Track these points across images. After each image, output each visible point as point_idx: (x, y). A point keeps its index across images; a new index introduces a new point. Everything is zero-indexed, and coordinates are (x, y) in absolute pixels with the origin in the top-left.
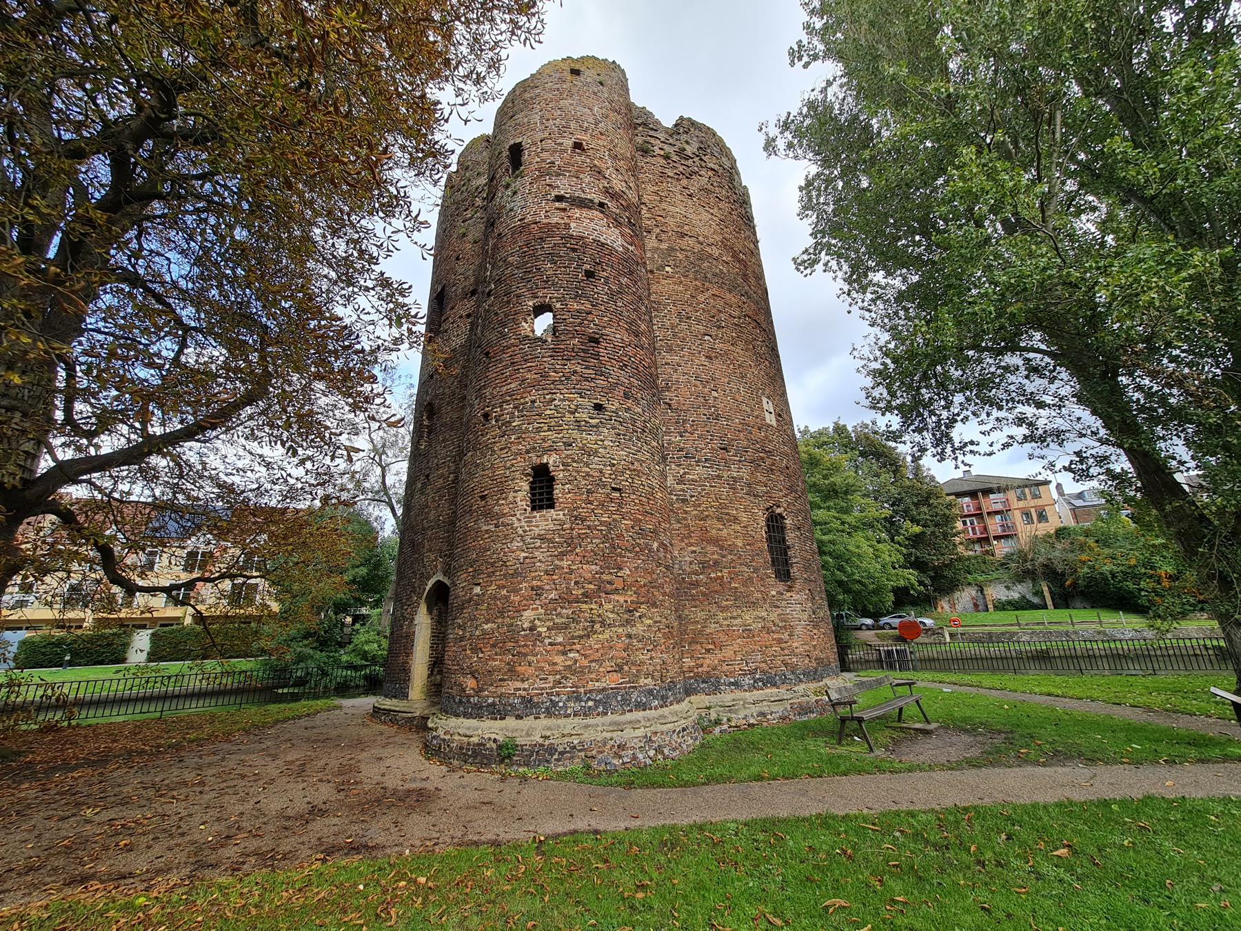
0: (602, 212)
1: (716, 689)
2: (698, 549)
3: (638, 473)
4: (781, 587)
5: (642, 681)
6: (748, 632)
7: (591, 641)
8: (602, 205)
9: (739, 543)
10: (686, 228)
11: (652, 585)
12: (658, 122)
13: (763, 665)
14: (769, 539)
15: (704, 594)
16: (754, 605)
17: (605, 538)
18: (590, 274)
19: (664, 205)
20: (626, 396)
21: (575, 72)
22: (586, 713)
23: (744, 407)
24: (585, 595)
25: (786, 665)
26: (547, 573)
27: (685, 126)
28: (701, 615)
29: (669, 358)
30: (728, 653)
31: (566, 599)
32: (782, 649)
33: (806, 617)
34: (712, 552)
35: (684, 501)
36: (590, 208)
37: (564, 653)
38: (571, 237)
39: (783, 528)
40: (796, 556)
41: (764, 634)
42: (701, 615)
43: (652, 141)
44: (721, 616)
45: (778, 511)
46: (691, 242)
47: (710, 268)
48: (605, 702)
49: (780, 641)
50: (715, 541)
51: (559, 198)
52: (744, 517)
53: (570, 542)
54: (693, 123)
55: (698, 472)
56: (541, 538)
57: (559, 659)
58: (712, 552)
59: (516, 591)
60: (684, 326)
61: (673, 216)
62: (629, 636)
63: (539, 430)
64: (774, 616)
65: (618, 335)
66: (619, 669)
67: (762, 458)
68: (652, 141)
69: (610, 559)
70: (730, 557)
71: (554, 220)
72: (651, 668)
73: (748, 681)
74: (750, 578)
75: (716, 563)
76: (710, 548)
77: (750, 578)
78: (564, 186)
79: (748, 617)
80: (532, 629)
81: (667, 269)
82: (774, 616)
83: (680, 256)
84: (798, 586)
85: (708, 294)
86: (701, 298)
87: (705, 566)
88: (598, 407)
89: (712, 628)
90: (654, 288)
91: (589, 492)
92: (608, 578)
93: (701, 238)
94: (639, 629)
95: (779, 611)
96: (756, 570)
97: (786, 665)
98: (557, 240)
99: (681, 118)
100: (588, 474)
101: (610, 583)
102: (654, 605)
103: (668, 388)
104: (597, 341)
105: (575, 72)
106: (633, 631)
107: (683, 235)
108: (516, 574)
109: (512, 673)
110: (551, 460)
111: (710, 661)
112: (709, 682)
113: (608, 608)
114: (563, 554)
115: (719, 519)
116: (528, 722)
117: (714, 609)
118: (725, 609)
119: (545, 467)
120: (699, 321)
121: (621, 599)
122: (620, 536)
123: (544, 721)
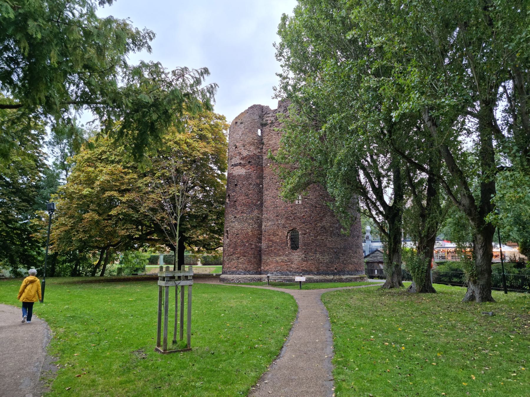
3: (243, 230)
6: (277, 262)
9: (278, 241)
11: (245, 252)
14: (291, 239)
16: (280, 256)
17: (235, 244)
18: (236, 185)
19: (269, 142)
20: (242, 213)
21: (236, 123)
22: (230, 274)
25: (287, 270)
28: (266, 258)
29: (266, 193)
30: (271, 266)
41: (282, 263)
42: (266, 258)
43: (268, 119)
48: (233, 273)
49: (287, 265)
50: (271, 241)
52: (280, 234)
53: (230, 245)
55: (270, 223)
66: (235, 267)
67: (290, 216)
68: (268, 119)
69: (235, 248)
73: (275, 273)
75: (271, 246)
77: (280, 250)
78: (234, 161)
79: (277, 259)
82: (286, 258)
84: (298, 250)
87: (268, 247)
88: (235, 217)
89: (268, 261)
90: (264, 172)
94: (240, 261)
96: (282, 247)
97: (287, 270)
102: (245, 256)
103: (265, 202)
105: (236, 123)
110: (228, 229)
111: (267, 268)
112: (266, 272)
113: (234, 257)
115: (273, 235)
118: (272, 257)
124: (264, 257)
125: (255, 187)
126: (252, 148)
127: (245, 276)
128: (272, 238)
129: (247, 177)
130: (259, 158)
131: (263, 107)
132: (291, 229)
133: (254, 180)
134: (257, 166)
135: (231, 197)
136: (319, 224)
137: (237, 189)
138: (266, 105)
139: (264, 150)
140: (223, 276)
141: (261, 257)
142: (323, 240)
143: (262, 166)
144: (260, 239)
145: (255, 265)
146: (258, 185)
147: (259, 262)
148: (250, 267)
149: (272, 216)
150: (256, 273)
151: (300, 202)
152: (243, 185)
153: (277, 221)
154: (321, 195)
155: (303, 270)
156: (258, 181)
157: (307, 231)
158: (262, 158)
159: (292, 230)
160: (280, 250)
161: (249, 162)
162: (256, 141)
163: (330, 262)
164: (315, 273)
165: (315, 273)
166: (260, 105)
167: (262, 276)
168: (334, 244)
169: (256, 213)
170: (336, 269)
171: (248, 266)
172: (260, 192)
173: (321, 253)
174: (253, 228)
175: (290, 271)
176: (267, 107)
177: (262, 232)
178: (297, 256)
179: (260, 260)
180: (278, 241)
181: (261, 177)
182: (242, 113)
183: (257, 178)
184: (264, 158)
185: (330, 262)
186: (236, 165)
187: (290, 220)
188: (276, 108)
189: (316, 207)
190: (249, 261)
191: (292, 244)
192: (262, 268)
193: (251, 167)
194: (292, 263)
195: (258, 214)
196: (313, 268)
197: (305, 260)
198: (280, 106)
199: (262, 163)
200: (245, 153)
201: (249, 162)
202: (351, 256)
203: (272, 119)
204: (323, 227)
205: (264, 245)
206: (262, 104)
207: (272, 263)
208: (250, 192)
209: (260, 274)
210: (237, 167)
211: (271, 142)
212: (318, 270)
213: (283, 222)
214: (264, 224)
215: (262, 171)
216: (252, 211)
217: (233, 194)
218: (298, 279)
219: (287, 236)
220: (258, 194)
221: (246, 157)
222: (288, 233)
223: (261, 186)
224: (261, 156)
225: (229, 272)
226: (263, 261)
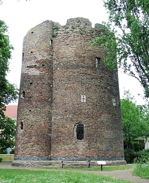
0: (35, 68)
1: (57, 160)
2: (56, 133)
4: (77, 140)
5: (34, 156)
6: (65, 150)
7: (26, 150)
8: (35, 66)
10: (64, 55)
12: (61, 25)
13: (68, 156)
14: (77, 131)
15: (57, 142)
17: (29, 134)
18: (31, 83)
20: (36, 107)
23: (74, 100)
24: (26, 143)
25: (75, 156)
26: (21, 140)
27: (70, 21)
29: (56, 92)
30: (60, 153)
31: (23, 144)
32: (74, 153)
33: (85, 147)
34: (59, 134)
35: (55, 124)
36: (32, 68)
37: (23, 151)
38: (29, 76)
39: (83, 128)
40: (85, 134)
41: (69, 150)
43: (58, 32)
44: (59, 146)
45: (82, 123)
46: (65, 59)
47: (70, 64)
48: (27, 159)
49: (74, 152)
51: (28, 67)
52: (68, 126)
54: (71, 20)
55: (59, 117)
56: (21, 134)
57: (22, 152)
58: (59, 134)
59: (18, 142)
60: (60, 83)
61: (61, 53)
62: (32, 149)
63: (21, 116)
64: (73, 147)
65: (36, 95)
67: (77, 112)
69: (30, 137)
70: (63, 135)
71: (26, 72)
72: (36, 154)
74: (68, 139)
75: (60, 136)
76: (59, 133)
79: (66, 147)
80: (19, 148)
81: (58, 69)
82: (73, 147)
83: (61, 64)
84: (83, 140)
85: (68, 72)
86: (65, 74)
87: (57, 137)
88: (30, 111)
91: (28, 126)
92: (29, 140)
93: (68, 57)
94: (34, 148)
95: (75, 146)
97: (75, 156)
98: (26, 77)
99: (68, 20)
100: (27, 123)
101: (30, 141)
103: (55, 99)
104: (31, 97)
105: (32, 32)
106: (33, 149)
107: (62, 58)
108: (18, 140)
109: (17, 154)
111: (56, 155)
113: (29, 145)
114: (23, 137)
116: (18, 160)
117: (58, 145)
119: (22, 122)
120: (64, 81)
121: (31, 143)
122: (32, 133)
123: (20, 161)
124: (54, 146)
125: (47, 86)
126: (46, 54)
127: (38, 161)
128: (61, 129)
129: (41, 78)
130: (51, 62)
131: (53, 23)
132: (78, 122)
133: (46, 81)
134: (49, 69)
135: (26, 94)
136: (99, 119)
137: (32, 87)
138: (56, 22)
139: (54, 57)
140: (14, 162)
141: (50, 145)
142: (101, 132)
143: (52, 69)
144: (50, 130)
145: (47, 152)
146: (49, 84)
147: (49, 149)
148: (42, 154)
149: (60, 111)
150: (47, 159)
151: (85, 101)
152: (38, 84)
153: (66, 115)
154: (101, 96)
155: (87, 156)
156: (49, 82)
157: (90, 124)
158: (52, 63)
159: (78, 123)
160: (68, 139)
161: (43, 65)
162: (49, 49)
163: (106, 150)
164: (96, 158)
165: (96, 158)
166: (52, 21)
167: (51, 161)
168: (109, 136)
169: (47, 108)
170: (110, 155)
171: (41, 153)
172: (51, 91)
173: (100, 142)
174: (45, 120)
175: (77, 157)
176: (58, 24)
177: (51, 124)
178: (82, 145)
179: (50, 148)
180: (66, 132)
181: (51, 79)
182: (38, 25)
183: (49, 79)
184: (54, 64)
185: (106, 150)
186: (31, 67)
187: (76, 116)
188: (65, 25)
189: (97, 105)
190: (42, 149)
191: (77, 135)
192: (52, 154)
193: (45, 69)
194: (78, 151)
195: (50, 109)
196: (95, 155)
197: (89, 148)
198: (68, 24)
199: (52, 67)
200: (40, 58)
201: (43, 65)
202: (119, 145)
203: (62, 32)
204: (102, 122)
205: (53, 135)
206: (53, 21)
207: (61, 150)
208: (43, 90)
209: (50, 160)
210: (32, 69)
211: (61, 51)
212: (98, 156)
213: (71, 116)
214: (53, 118)
215: (53, 73)
216: (45, 106)
217: (28, 91)
218: (100, 162)
219: (74, 128)
220: (49, 93)
221: (40, 61)
222: (75, 125)
223: (51, 86)
224: (52, 61)
225: (23, 157)
226: (53, 149)
